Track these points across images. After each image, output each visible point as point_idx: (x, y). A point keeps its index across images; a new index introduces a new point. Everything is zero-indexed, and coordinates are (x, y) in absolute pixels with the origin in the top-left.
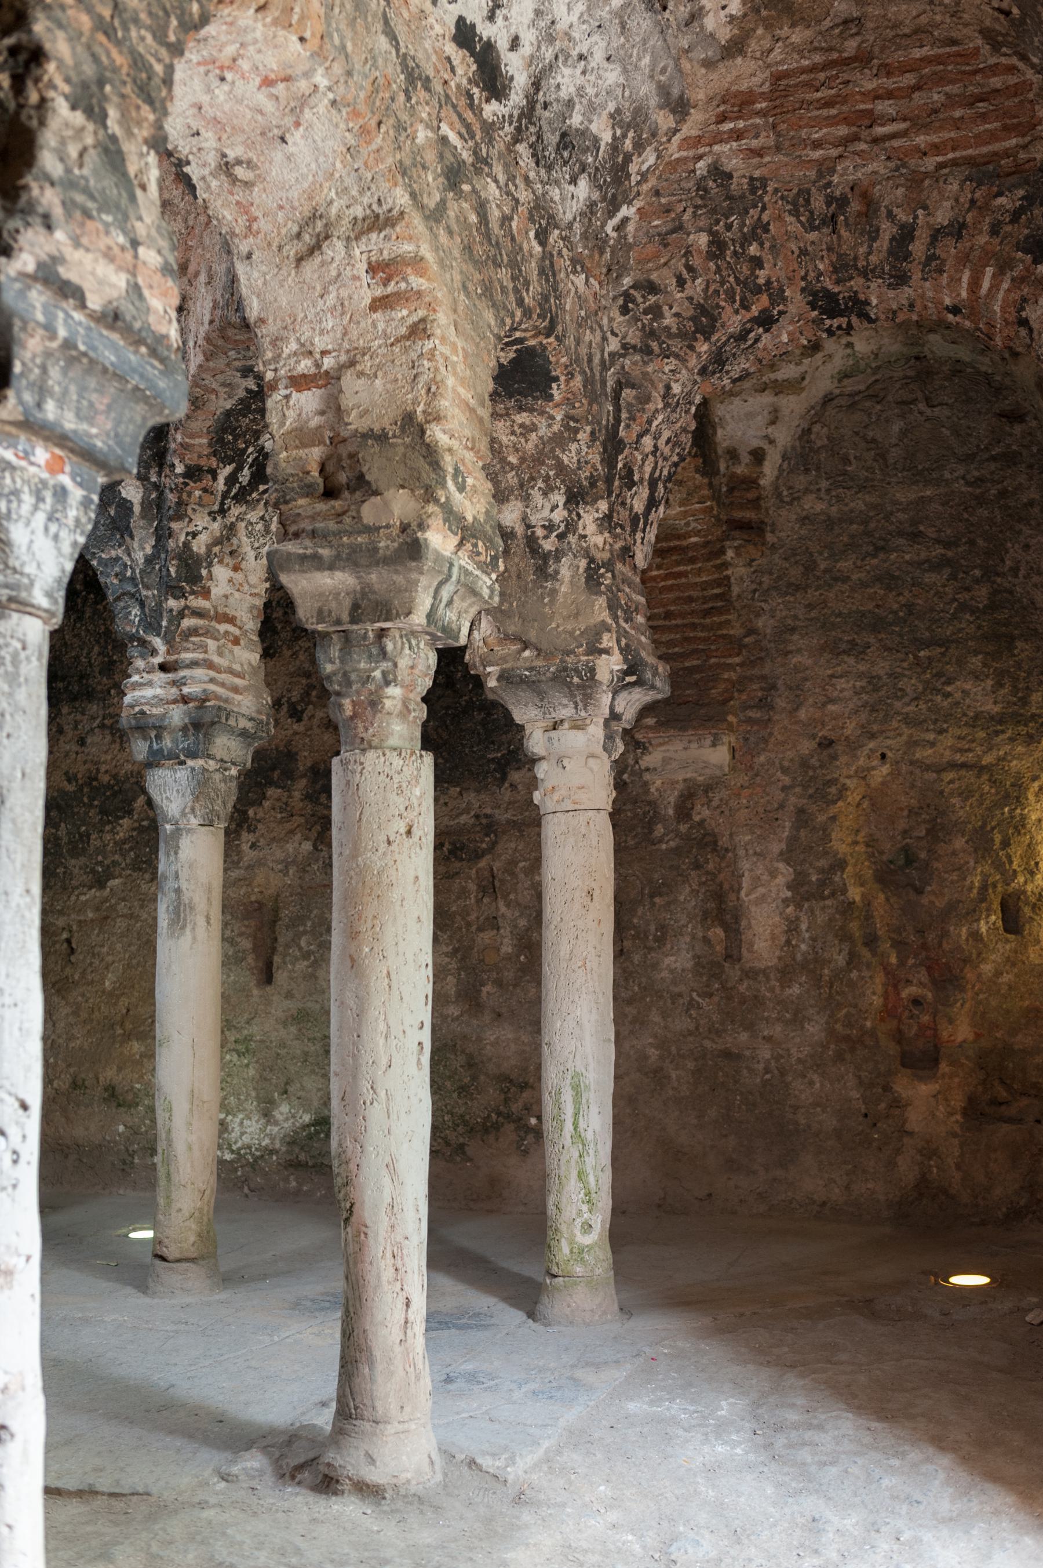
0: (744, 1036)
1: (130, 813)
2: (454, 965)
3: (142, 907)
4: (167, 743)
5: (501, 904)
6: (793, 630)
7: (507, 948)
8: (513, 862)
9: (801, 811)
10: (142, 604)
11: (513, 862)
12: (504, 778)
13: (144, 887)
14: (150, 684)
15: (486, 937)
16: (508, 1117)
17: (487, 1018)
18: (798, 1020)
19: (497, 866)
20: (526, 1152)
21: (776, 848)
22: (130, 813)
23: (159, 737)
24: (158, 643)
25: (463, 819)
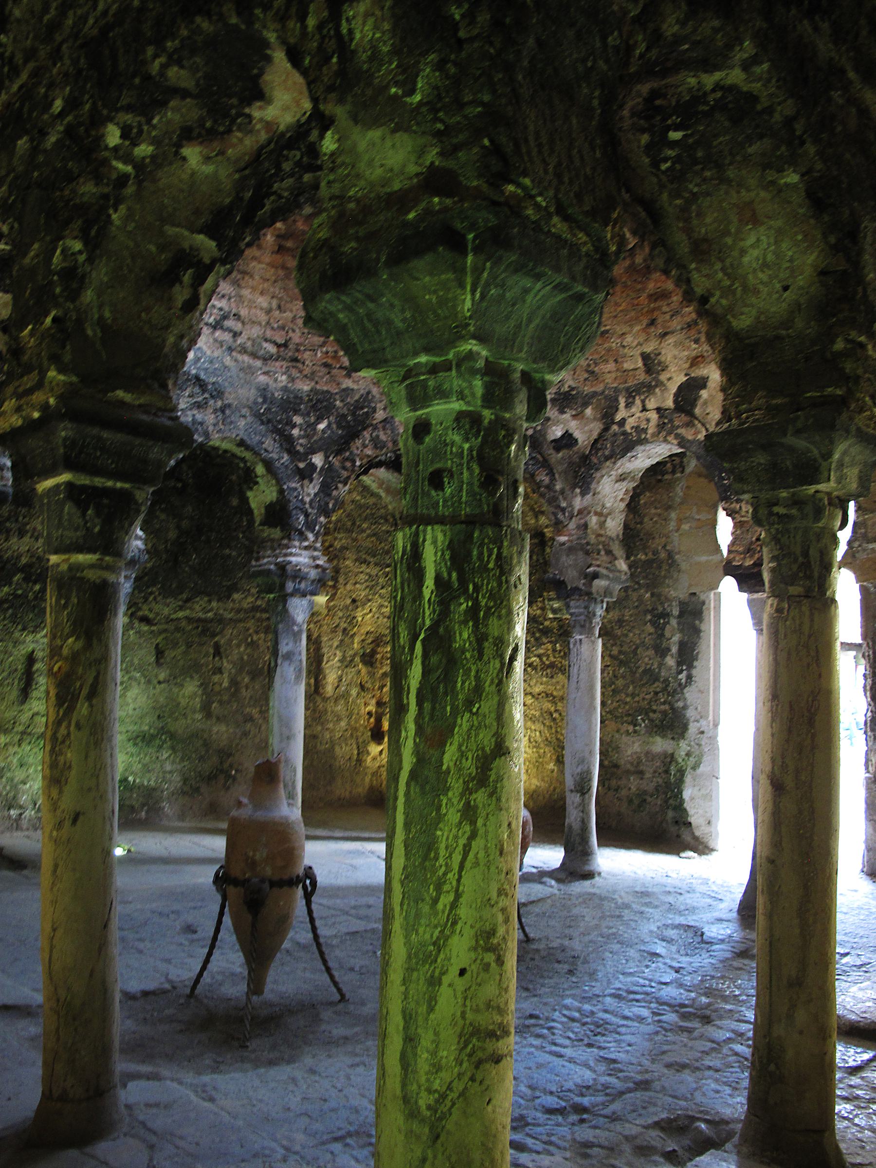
0: (319, 728)
1: (10, 585)
2: (200, 692)
3: (14, 647)
4: (303, 585)
5: (225, 661)
6: (347, 549)
7: (226, 684)
8: (230, 640)
9: (345, 629)
10: (307, 515)
11: (230, 640)
12: (229, 597)
13: (17, 634)
14: (300, 555)
15: (216, 678)
16: (222, 771)
17: (214, 720)
18: (339, 719)
19: (222, 642)
20: (228, 788)
21: (336, 644)
22: (10, 585)
23: (300, 582)
24: (311, 537)
25: (210, 615)
